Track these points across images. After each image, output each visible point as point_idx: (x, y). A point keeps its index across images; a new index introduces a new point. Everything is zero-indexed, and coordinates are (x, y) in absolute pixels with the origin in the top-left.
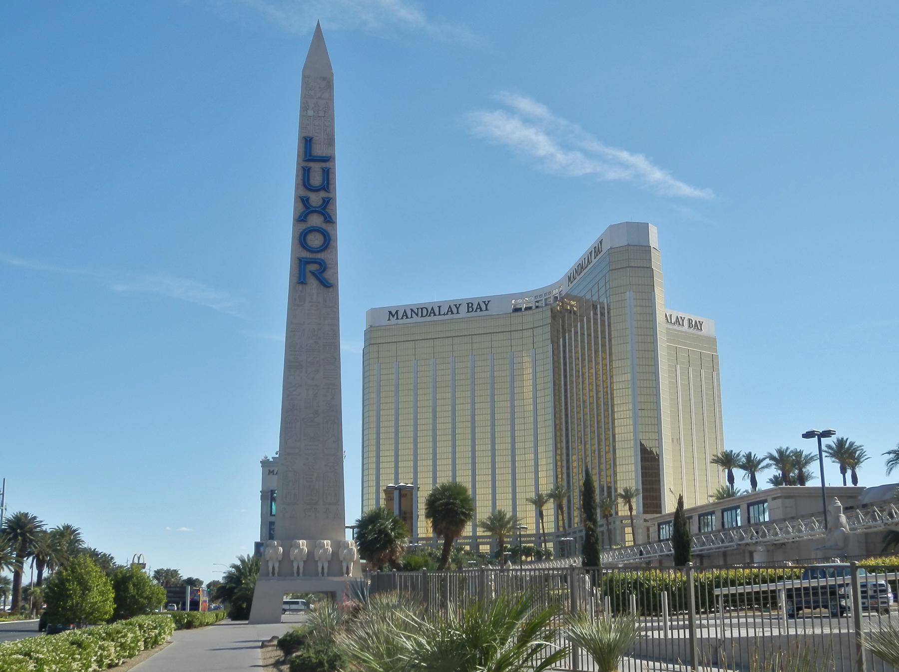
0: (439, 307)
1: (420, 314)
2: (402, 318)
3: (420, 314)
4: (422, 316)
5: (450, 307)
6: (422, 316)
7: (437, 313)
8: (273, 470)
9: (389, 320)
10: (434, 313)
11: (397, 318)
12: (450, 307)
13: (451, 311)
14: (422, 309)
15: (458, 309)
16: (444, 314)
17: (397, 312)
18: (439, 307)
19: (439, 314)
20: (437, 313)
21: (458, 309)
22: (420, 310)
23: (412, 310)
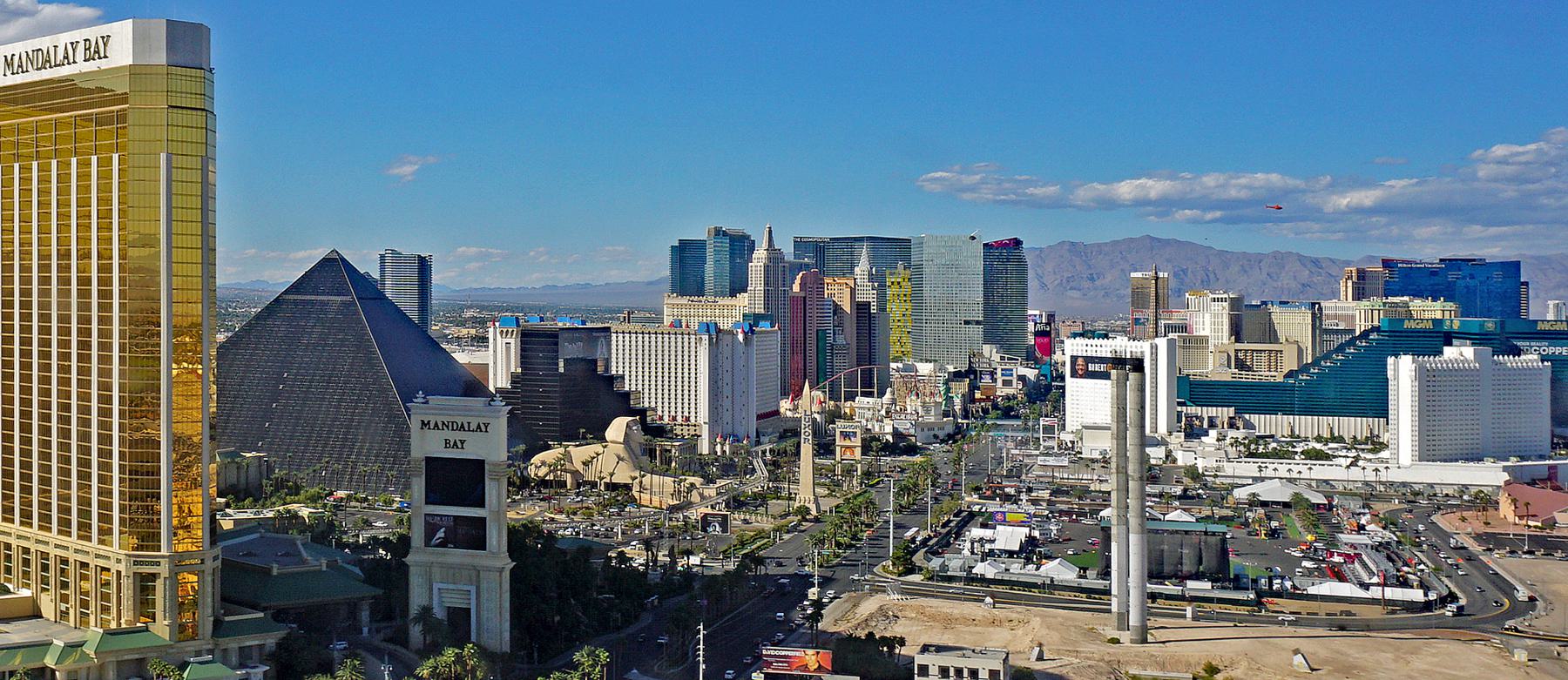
0: (469, 423)
1: (450, 428)
2: (434, 429)
3: (450, 428)
4: (453, 430)
5: (479, 425)
6: (453, 430)
7: (467, 429)
8: (429, 422)
9: (422, 428)
10: (464, 428)
11: (429, 428)
12: (479, 425)
13: (480, 428)
14: (453, 422)
15: (486, 427)
16: (473, 431)
17: (429, 422)
18: (469, 423)
19: (469, 430)
20: (467, 429)
21: (486, 427)
22: (450, 424)
23: (443, 422)
